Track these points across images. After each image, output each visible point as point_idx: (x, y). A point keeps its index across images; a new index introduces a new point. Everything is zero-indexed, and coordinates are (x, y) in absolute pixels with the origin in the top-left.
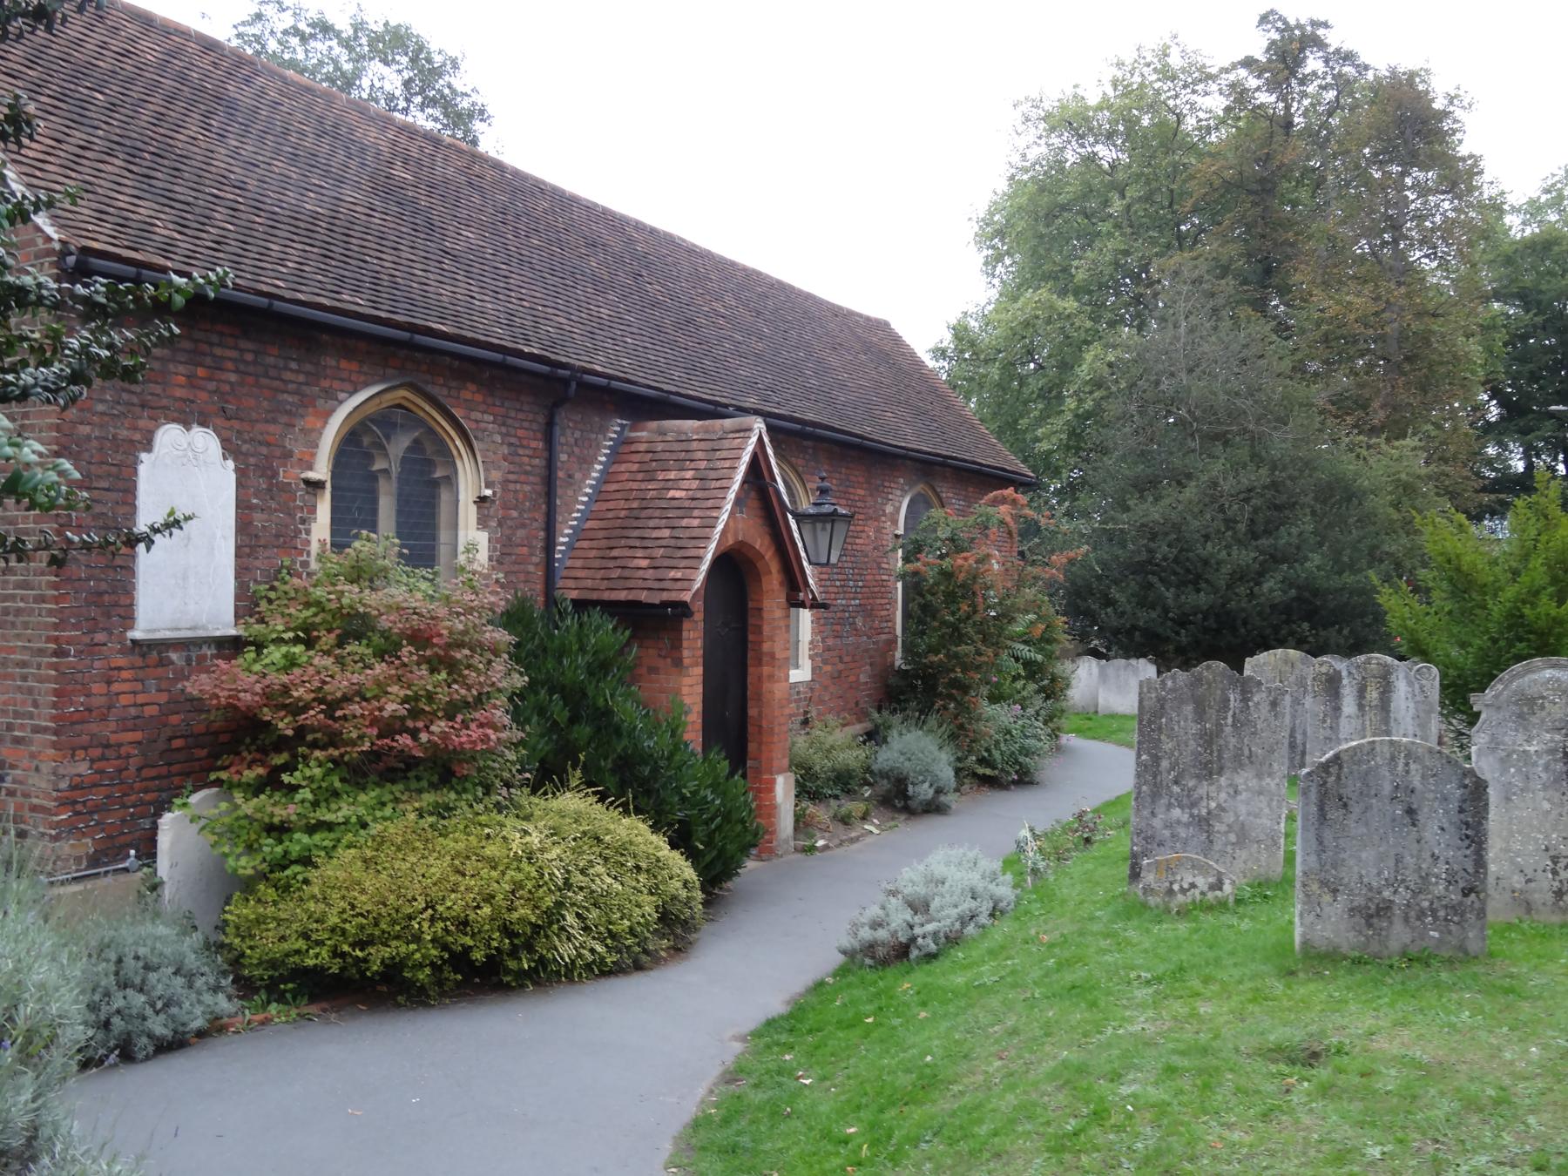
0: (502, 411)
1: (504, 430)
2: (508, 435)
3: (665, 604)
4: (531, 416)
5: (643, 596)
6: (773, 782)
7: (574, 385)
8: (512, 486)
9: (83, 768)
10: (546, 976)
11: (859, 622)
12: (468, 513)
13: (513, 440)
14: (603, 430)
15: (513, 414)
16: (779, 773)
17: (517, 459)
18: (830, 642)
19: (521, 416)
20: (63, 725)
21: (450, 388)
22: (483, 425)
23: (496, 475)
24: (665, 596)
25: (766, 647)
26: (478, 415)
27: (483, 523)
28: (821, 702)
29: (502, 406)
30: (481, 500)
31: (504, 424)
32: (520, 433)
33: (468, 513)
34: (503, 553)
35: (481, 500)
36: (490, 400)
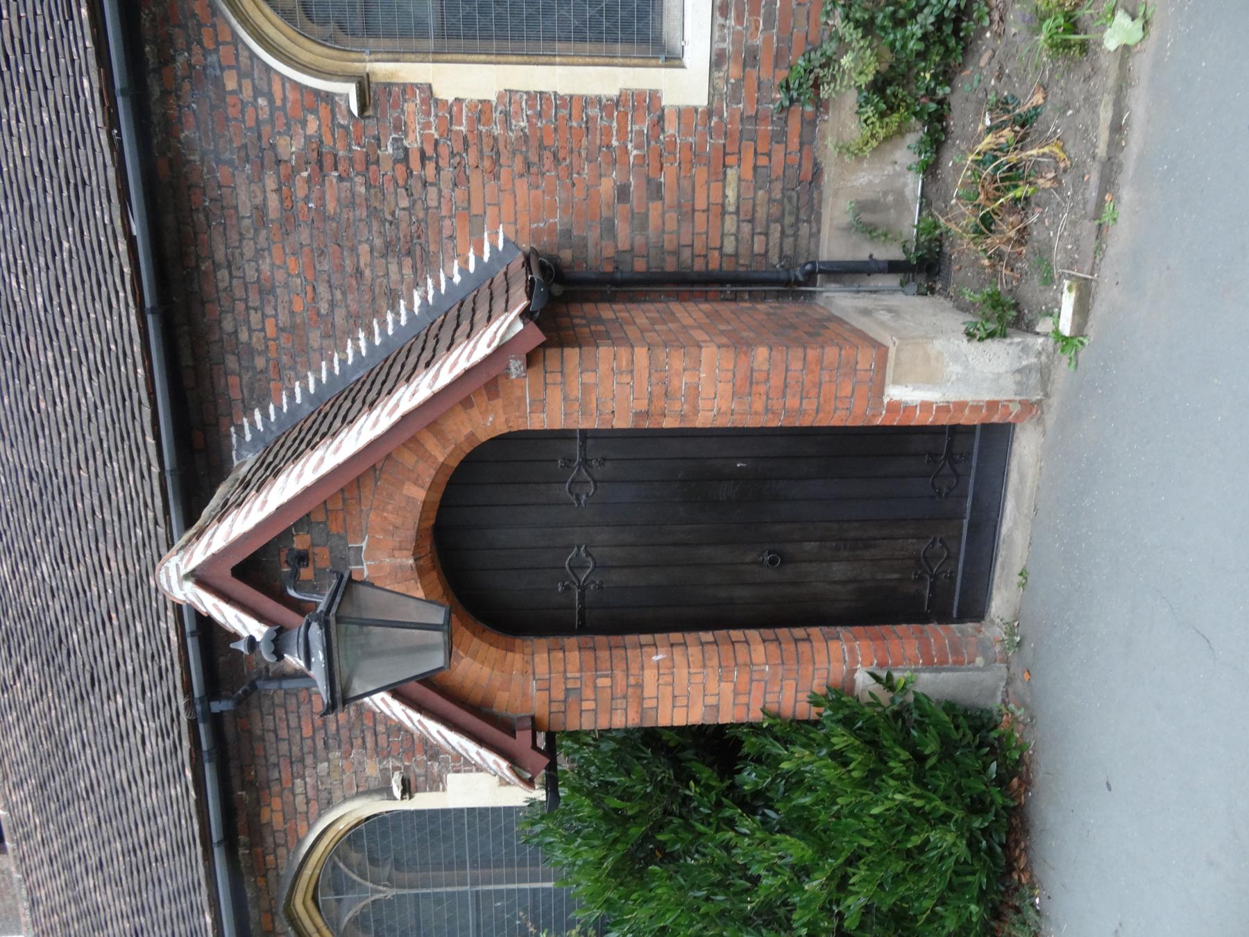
0: (284, 764)
1: (309, 760)
2: (314, 752)
4: (280, 712)
6: (894, 407)
7: (216, 707)
8: (382, 741)
13: (320, 744)
15: (284, 747)
16: (880, 392)
17: (344, 733)
19: (283, 733)
21: (277, 845)
22: (311, 794)
23: (372, 769)
25: (622, 422)
26: (300, 800)
29: (277, 765)
30: (407, 790)
31: (302, 760)
32: (307, 732)
36: (276, 788)
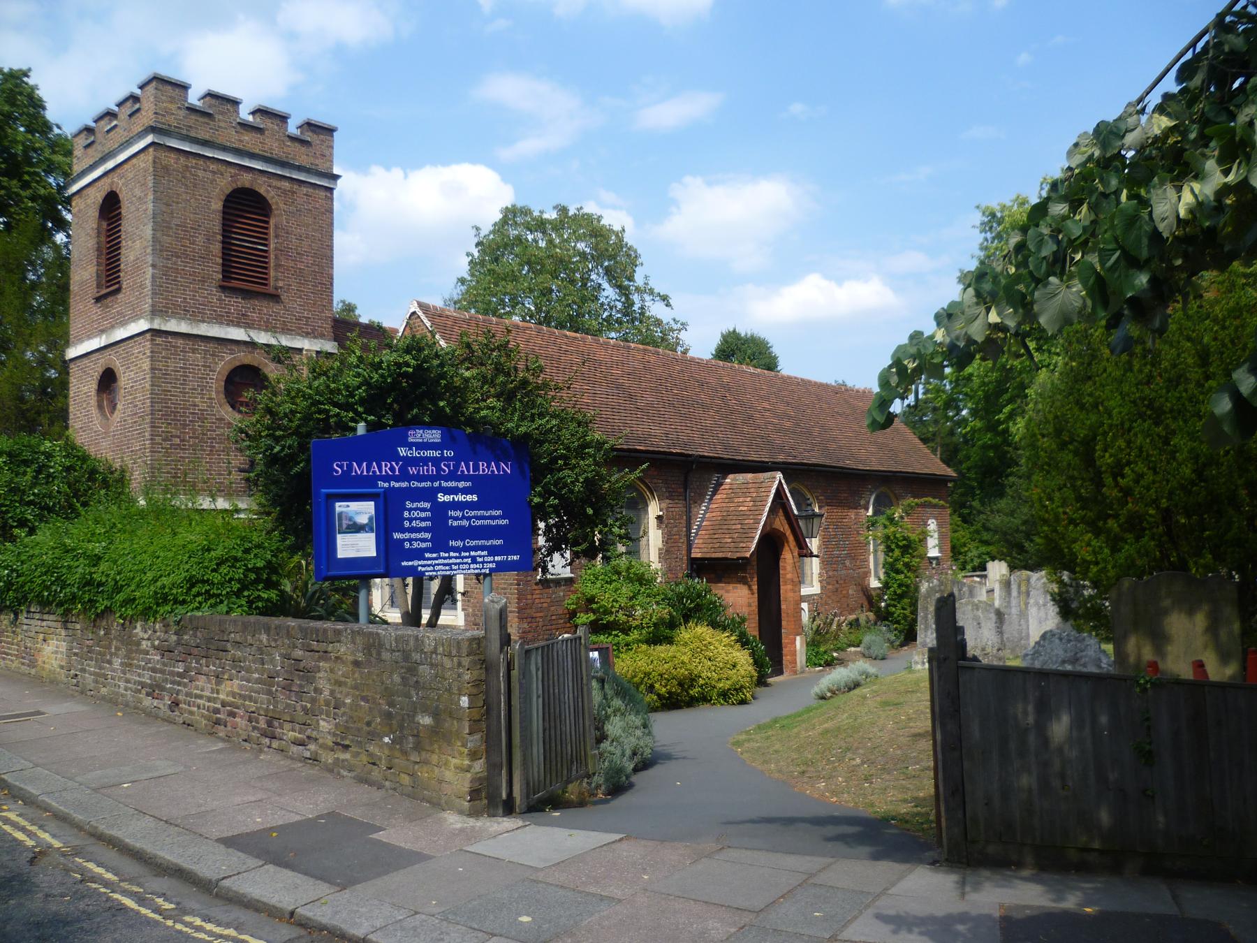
3: (738, 559)
5: (729, 555)
9: (526, 626)
10: (692, 702)
11: (847, 563)
12: (652, 522)
14: (710, 480)
18: (831, 573)
20: (520, 610)
23: (664, 505)
24: (738, 555)
27: (659, 527)
28: (826, 604)
33: (652, 522)
34: (668, 539)
35: (659, 518)
